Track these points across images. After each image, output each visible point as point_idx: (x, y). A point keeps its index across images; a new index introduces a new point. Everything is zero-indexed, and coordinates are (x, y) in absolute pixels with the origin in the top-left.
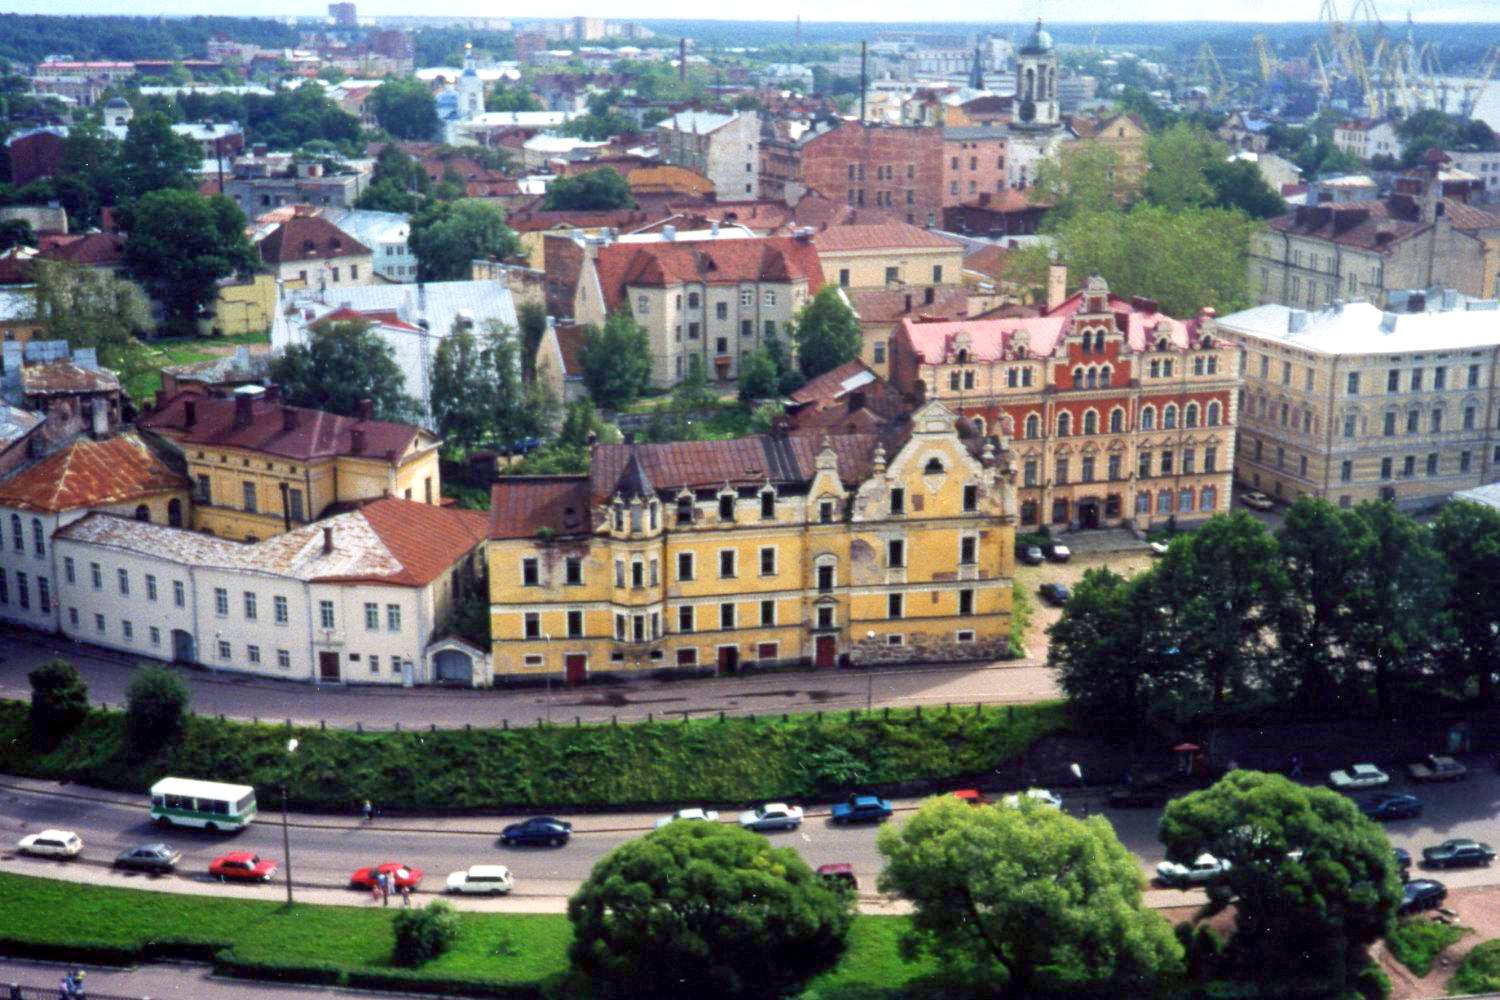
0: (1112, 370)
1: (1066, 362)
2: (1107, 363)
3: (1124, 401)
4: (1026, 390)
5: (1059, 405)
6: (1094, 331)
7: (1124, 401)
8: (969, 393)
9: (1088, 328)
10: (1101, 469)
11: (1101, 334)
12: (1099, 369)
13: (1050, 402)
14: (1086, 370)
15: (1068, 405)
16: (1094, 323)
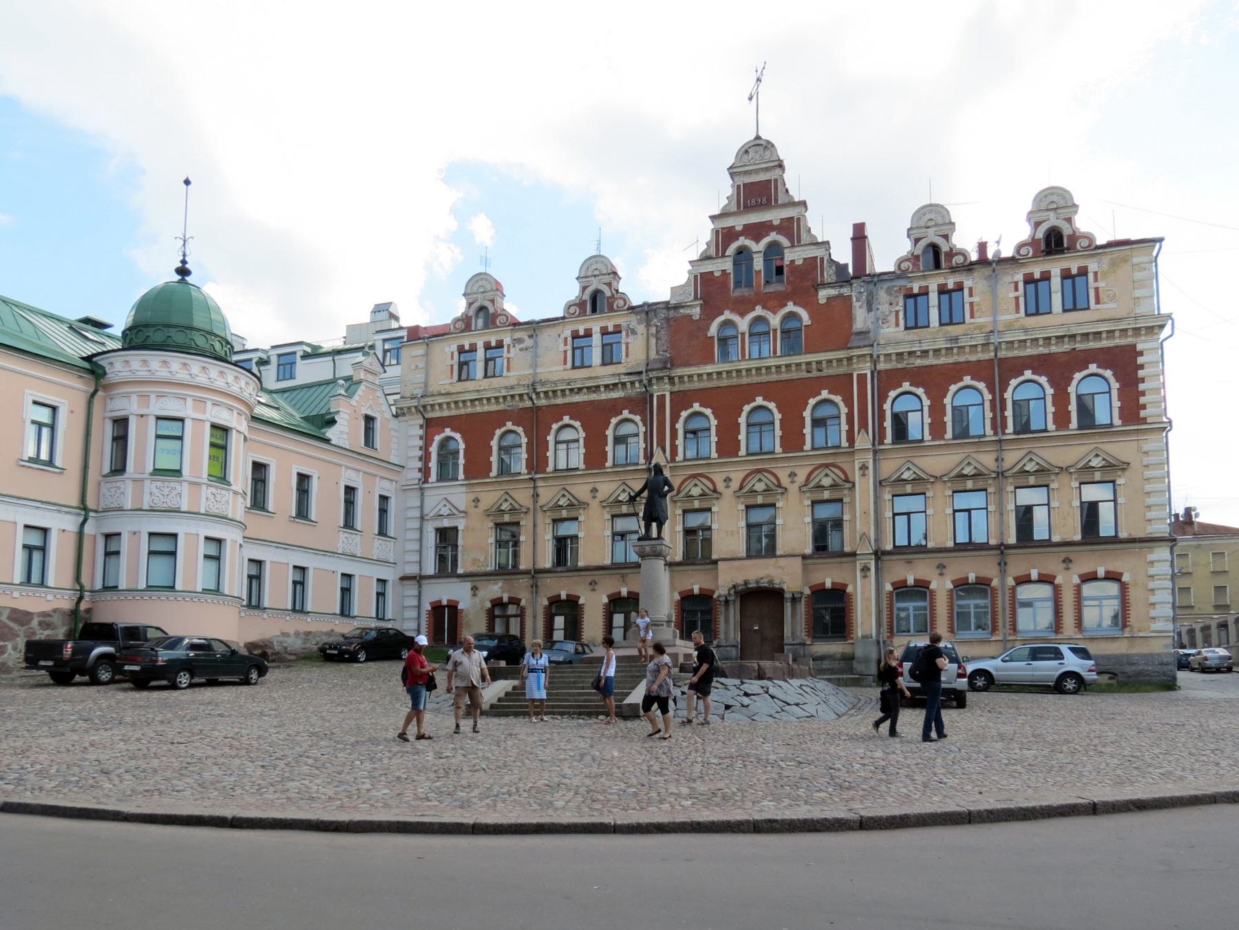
0: (804, 315)
1: (696, 312)
2: (791, 307)
3: (841, 384)
4: (610, 369)
5: (681, 400)
6: (758, 247)
7: (841, 384)
8: (495, 382)
9: (743, 241)
10: (795, 531)
11: (774, 250)
12: (775, 320)
13: (662, 390)
14: (743, 324)
15: (705, 396)
16: (756, 231)
